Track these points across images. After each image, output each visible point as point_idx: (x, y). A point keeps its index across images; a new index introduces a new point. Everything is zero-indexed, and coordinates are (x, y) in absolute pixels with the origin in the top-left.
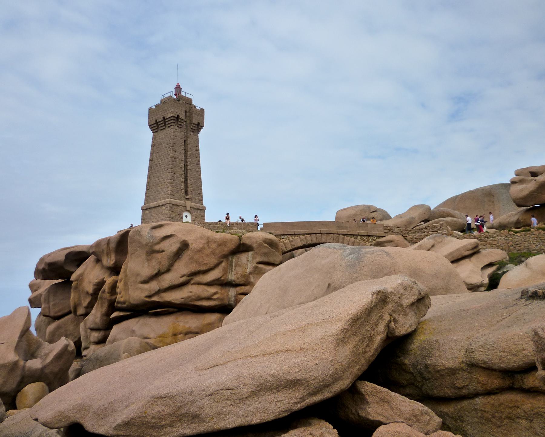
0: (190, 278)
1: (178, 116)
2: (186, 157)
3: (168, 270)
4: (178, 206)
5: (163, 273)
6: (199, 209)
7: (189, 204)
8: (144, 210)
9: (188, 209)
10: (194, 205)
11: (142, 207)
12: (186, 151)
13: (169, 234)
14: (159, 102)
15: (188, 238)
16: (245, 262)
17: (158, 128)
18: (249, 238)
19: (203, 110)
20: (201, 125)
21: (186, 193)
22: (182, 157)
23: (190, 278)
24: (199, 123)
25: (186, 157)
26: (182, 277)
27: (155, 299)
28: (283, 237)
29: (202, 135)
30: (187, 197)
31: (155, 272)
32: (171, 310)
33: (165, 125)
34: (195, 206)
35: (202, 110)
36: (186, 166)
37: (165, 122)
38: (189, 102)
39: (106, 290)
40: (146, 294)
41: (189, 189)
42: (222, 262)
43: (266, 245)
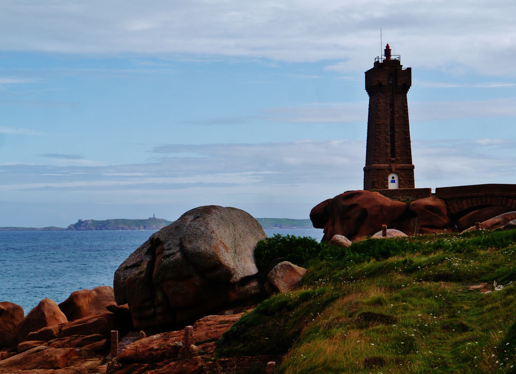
1: (380, 84)
2: (392, 120)
4: (383, 170)
6: (407, 169)
7: (394, 167)
8: (365, 169)
9: (394, 169)
10: (399, 165)
12: (393, 113)
13: (354, 203)
14: (372, 66)
15: (366, 206)
16: (413, 226)
18: (414, 204)
19: (409, 70)
22: (388, 122)
25: (392, 120)
29: (410, 95)
34: (401, 167)
35: (409, 70)
36: (392, 128)
38: (397, 62)
43: (427, 211)
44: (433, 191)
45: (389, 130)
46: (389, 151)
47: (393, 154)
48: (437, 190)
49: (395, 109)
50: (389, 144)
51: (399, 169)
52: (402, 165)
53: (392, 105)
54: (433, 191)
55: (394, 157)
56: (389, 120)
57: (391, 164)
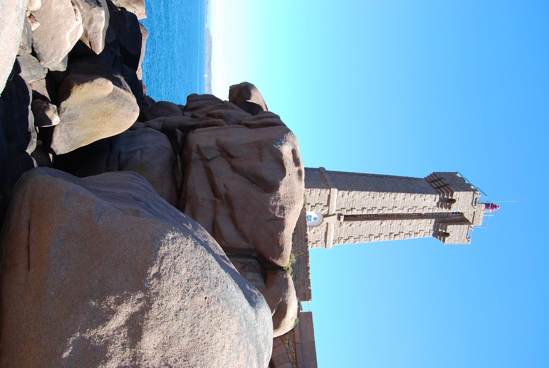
0: (224, 197)
3: (234, 169)
5: (230, 163)
6: (326, 238)
7: (332, 220)
9: (327, 220)
11: (323, 168)
17: (433, 182)
18: (287, 280)
20: (447, 239)
21: (348, 218)
22: (396, 211)
23: (224, 197)
24: (447, 235)
26: (225, 186)
27: (194, 155)
28: (291, 343)
30: (342, 218)
31: (232, 153)
32: (179, 179)
33: (439, 188)
37: (442, 187)
39: (209, 120)
40: (202, 144)
41: (356, 223)
42: (248, 241)
44: (306, 306)
45: (386, 213)
46: (355, 212)
47: (348, 218)
48: (309, 315)
49: (415, 221)
50: (365, 212)
51: (327, 228)
52: (333, 231)
53: (420, 216)
54: (306, 306)
55: (345, 220)
56: (400, 212)
57: (336, 217)
